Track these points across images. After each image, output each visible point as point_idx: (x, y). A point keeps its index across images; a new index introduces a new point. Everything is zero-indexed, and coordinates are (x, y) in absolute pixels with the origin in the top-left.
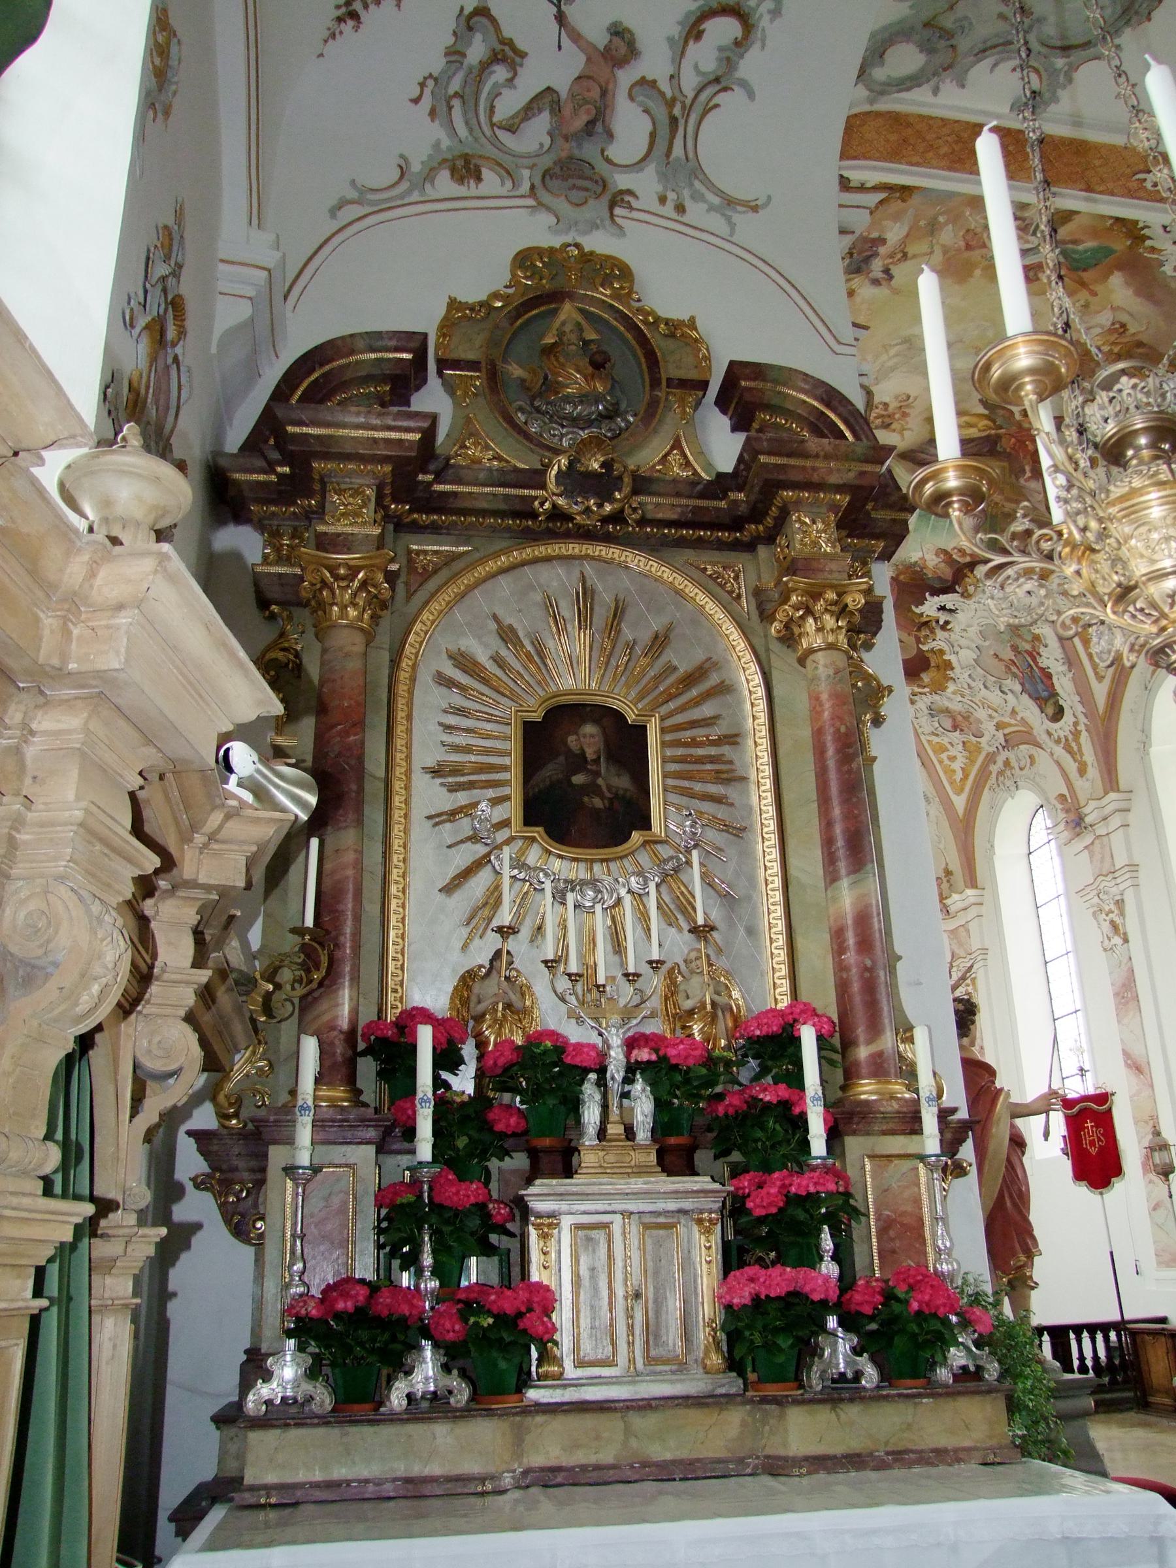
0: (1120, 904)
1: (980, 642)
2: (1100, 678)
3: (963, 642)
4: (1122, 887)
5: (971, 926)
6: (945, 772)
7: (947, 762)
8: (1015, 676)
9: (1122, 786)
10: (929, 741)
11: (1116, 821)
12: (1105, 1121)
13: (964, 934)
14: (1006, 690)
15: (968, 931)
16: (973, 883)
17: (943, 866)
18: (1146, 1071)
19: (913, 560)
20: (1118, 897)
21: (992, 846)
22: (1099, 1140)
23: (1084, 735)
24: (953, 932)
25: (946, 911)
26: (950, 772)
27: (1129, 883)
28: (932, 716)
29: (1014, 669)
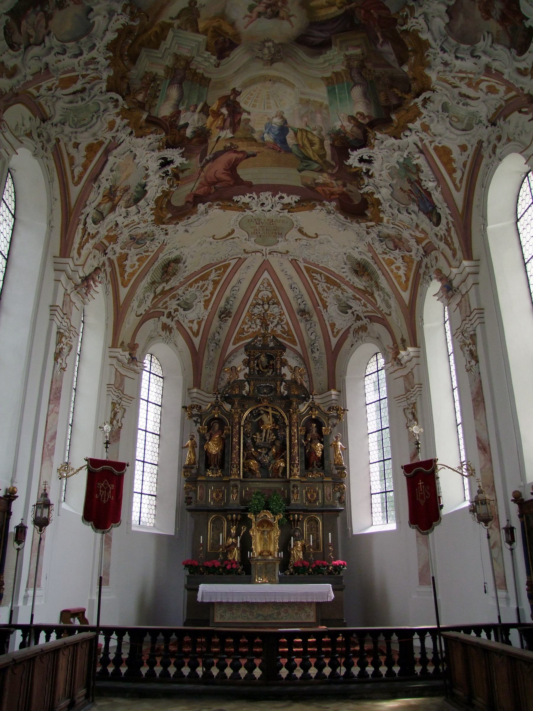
0: (473, 337)
1: (391, 182)
2: (458, 189)
3: (382, 184)
4: (474, 325)
5: (415, 371)
6: (396, 278)
7: (395, 271)
8: (414, 201)
9: (475, 257)
10: (383, 259)
11: (470, 280)
13: (411, 377)
14: (410, 211)
15: (413, 375)
16: (415, 344)
17: (401, 337)
18: (488, 450)
19: (338, 128)
20: (472, 333)
21: (422, 320)
23: (453, 229)
24: (406, 377)
26: (398, 277)
27: (477, 322)
28: (381, 241)
29: (413, 197)
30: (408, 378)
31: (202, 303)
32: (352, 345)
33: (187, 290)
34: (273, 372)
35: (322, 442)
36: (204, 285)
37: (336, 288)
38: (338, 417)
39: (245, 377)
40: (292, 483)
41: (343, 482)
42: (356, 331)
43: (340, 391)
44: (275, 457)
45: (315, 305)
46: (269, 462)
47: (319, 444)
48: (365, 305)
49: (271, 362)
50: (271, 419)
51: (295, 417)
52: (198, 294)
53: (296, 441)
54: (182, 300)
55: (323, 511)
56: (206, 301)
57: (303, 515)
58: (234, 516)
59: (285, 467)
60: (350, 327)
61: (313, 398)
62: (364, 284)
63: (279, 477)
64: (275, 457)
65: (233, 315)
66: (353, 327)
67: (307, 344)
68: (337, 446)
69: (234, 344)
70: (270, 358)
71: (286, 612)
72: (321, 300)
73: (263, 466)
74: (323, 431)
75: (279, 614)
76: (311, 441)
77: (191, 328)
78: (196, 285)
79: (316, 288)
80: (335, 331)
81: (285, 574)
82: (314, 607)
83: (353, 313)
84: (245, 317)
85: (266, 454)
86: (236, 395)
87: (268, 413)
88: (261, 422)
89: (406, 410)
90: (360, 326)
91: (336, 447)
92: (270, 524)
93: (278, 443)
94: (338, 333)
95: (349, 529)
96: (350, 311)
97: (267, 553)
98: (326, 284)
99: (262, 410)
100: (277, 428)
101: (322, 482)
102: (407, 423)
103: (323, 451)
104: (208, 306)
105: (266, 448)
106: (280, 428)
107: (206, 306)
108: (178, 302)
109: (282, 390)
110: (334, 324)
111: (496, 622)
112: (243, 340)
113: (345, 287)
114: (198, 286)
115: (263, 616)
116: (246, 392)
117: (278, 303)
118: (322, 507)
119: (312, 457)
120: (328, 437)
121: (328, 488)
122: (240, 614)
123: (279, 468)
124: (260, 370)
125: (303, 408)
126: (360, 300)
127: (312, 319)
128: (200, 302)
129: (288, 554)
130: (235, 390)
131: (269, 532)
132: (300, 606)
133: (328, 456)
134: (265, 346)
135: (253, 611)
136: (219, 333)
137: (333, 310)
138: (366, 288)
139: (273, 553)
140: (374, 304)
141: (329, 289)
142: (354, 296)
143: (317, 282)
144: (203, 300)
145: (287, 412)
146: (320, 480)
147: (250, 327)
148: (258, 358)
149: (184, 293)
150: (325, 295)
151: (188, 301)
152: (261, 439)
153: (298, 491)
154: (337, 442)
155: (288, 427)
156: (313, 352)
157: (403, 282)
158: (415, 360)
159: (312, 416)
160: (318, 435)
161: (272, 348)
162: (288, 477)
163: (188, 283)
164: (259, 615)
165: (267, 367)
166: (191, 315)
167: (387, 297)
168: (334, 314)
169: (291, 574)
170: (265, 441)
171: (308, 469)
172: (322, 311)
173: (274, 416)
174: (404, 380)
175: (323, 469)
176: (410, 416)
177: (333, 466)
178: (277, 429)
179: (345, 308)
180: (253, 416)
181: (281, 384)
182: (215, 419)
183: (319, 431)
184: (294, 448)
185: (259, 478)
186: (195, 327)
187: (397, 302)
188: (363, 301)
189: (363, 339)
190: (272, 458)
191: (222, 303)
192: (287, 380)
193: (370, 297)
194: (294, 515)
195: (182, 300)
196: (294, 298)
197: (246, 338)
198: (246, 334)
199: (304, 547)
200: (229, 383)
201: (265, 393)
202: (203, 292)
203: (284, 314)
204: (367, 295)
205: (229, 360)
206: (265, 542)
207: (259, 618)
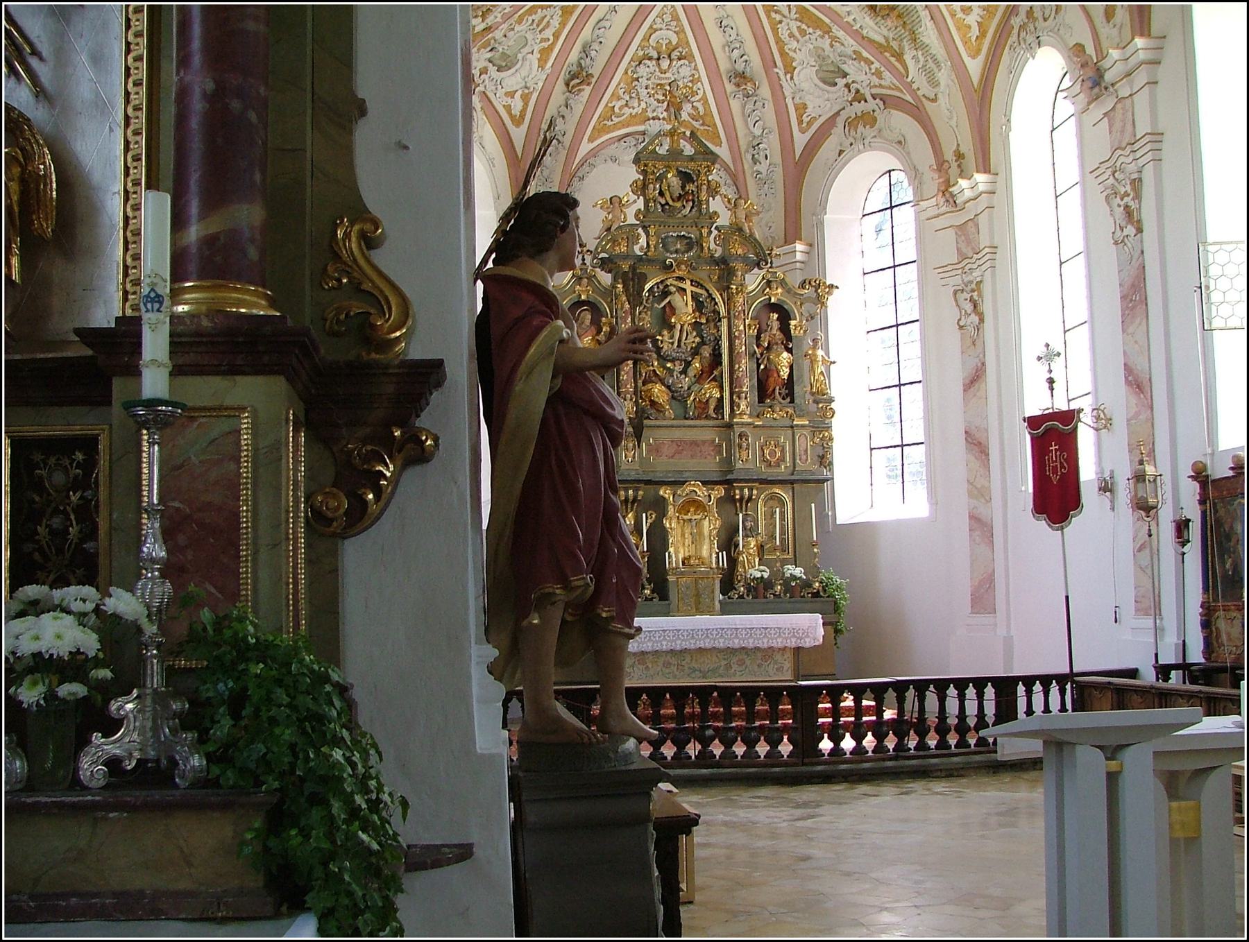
5: (983, 220)
6: (958, 29)
7: (960, 15)
12: (1068, 443)
13: (973, 230)
15: (977, 226)
17: (955, 147)
21: (1009, 121)
22: (1062, 466)
24: (961, 228)
25: (951, 200)
30: (965, 231)
31: (537, 55)
32: (841, 152)
33: (513, 29)
34: (692, 208)
35: (790, 351)
36: (546, 16)
37: (819, 32)
38: (820, 301)
39: (636, 216)
40: (738, 430)
41: (829, 427)
42: (851, 124)
43: (811, 245)
44: (699, 378)
45: (769, 64)
46: (689, 388)
47: (785, 354)
48: (878, 74)
49: (690, 187)
50: (690, 302)
51: (741, 300)
52: (529, 36)
53: (744, 348)
54: (501, 50)
55: (792, 482)
56: (542, 51)
57: (757, 489)
58: (631, 492)
59: (721, 400)
60: (838, 113)
61: (771, 263)
62: (885, 32)
63: (708, 417)
64: (699, 378)
65: (594, 80)
66: (844, 114)
67: (743, 143)
68: (815, 355)
69: (591, 140)
70: (686, 178)
71: (741, 663)
72: (783, 54)
73: (677, 397)
74: (792, 327)
75: (728, 667)
76: (768, 348)
77: (508, 108)
78: (530, 19)
79: (775, 31)
80: (805, 119)
81: (729, 598)
82: (789, 655)
83: (847, 86)
84: (619, 84)
85: (681, 373)
86: (626, 257)
87: (684, 290)
88: (671, 308)
89: (959, 294)
90: (859, 114)
91: (813, 361)
92: (699, 506)
93: (706, 352)
94: (810, 124)
95: (830, 513)
96: (841, 82)
97: (697, 561)
98: (799, 24)
99: (671, 285)
100: (704, 321)
101: (792, 427)
102: (960, 320)
103: (791, 368)
104: (546, 62)
105: (681, 361)
106: (707, 320)
107: (542, 63)
108: (489, 55)
109: (712, 246)
110: (805, 106)
111: (1067, 670)
112: (608, 133)
113: (841, 34)
114: (533, 20)
115: (700, 671)
116: (641, 249)
117: (688, 57)
118: (793, 474)
119: (771, 380)
120: (801, 339)
121: (803, 438)
122: (659, 669)
123: (707, 401)
124: (667, 204)
125: (753, 280)
126: (867, 61)
127: (758, 92)
128: (532, 52)
129: (733, 562)
130: (620, 244)
131: (699, 523)
132: (768, 653)
133: (801, 376)
134: (675, 154)
135: (683, 663)
136: (563, 117)
137: (806, 76)
138: (887, 39)
139: (707, 561)
140: (902, 75)
141: (803, 33)
142: (855, 52)
143: (778, 17)
144: (537, 48)
145: (725, 289)
146: (788, 423)
147: (626, 105)
148: (660, 179)
149: (505, 36)
150: (794, 44)
151: (508, 52)
152: (672, 343)
153: (748, 445)
154: (814, 347)
155: (725, 322)
156: (755, 161)
157: (974, 39)
158: (984, 201)
159: (770, 299)
160: (782, 336)
161: (691, 158)
162: (727, 417)
163: (517, 16)
164: (694, 670)
165: (680, 197)
166: (512, 80)
167: (931, 64)
168: (805, 86)
169: (741, 597)
170: (679, 346)
171: (763, 402)
172: (782, 77)
173: (695, 297)
174: (956, 233)
175: (792, 401)
176: (968, 307)
177: (808, 396)
178: (702, 324)
179: (831, 75)
180: (654, 296)
181: (710, 232)
182: (578, 304)
183: (785, 328)
184: (739, 363)
185: (670, 419)
186: (517, 105)
187: (954, 77)
188: (876, 65)
189: (866, 142)
190: (693, 380)
191: (574, 56)
192: (723, 226)
193: (893, 59)
194: (741, 489)
195: (501, 50)
196: (724, 47)
197: (616, 127)
198: (616, 120)
199: (761, 548)
200: (609, 229)
201: (677, 252)
202: (540, 32)
203: (699, 80)
204: (887, 54)
205: (580, 174)
206: (697, 539)
207: (693, 675)
